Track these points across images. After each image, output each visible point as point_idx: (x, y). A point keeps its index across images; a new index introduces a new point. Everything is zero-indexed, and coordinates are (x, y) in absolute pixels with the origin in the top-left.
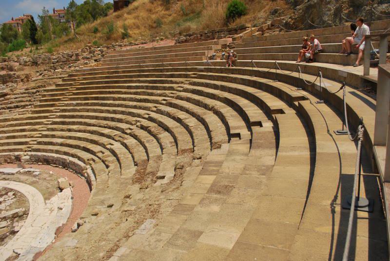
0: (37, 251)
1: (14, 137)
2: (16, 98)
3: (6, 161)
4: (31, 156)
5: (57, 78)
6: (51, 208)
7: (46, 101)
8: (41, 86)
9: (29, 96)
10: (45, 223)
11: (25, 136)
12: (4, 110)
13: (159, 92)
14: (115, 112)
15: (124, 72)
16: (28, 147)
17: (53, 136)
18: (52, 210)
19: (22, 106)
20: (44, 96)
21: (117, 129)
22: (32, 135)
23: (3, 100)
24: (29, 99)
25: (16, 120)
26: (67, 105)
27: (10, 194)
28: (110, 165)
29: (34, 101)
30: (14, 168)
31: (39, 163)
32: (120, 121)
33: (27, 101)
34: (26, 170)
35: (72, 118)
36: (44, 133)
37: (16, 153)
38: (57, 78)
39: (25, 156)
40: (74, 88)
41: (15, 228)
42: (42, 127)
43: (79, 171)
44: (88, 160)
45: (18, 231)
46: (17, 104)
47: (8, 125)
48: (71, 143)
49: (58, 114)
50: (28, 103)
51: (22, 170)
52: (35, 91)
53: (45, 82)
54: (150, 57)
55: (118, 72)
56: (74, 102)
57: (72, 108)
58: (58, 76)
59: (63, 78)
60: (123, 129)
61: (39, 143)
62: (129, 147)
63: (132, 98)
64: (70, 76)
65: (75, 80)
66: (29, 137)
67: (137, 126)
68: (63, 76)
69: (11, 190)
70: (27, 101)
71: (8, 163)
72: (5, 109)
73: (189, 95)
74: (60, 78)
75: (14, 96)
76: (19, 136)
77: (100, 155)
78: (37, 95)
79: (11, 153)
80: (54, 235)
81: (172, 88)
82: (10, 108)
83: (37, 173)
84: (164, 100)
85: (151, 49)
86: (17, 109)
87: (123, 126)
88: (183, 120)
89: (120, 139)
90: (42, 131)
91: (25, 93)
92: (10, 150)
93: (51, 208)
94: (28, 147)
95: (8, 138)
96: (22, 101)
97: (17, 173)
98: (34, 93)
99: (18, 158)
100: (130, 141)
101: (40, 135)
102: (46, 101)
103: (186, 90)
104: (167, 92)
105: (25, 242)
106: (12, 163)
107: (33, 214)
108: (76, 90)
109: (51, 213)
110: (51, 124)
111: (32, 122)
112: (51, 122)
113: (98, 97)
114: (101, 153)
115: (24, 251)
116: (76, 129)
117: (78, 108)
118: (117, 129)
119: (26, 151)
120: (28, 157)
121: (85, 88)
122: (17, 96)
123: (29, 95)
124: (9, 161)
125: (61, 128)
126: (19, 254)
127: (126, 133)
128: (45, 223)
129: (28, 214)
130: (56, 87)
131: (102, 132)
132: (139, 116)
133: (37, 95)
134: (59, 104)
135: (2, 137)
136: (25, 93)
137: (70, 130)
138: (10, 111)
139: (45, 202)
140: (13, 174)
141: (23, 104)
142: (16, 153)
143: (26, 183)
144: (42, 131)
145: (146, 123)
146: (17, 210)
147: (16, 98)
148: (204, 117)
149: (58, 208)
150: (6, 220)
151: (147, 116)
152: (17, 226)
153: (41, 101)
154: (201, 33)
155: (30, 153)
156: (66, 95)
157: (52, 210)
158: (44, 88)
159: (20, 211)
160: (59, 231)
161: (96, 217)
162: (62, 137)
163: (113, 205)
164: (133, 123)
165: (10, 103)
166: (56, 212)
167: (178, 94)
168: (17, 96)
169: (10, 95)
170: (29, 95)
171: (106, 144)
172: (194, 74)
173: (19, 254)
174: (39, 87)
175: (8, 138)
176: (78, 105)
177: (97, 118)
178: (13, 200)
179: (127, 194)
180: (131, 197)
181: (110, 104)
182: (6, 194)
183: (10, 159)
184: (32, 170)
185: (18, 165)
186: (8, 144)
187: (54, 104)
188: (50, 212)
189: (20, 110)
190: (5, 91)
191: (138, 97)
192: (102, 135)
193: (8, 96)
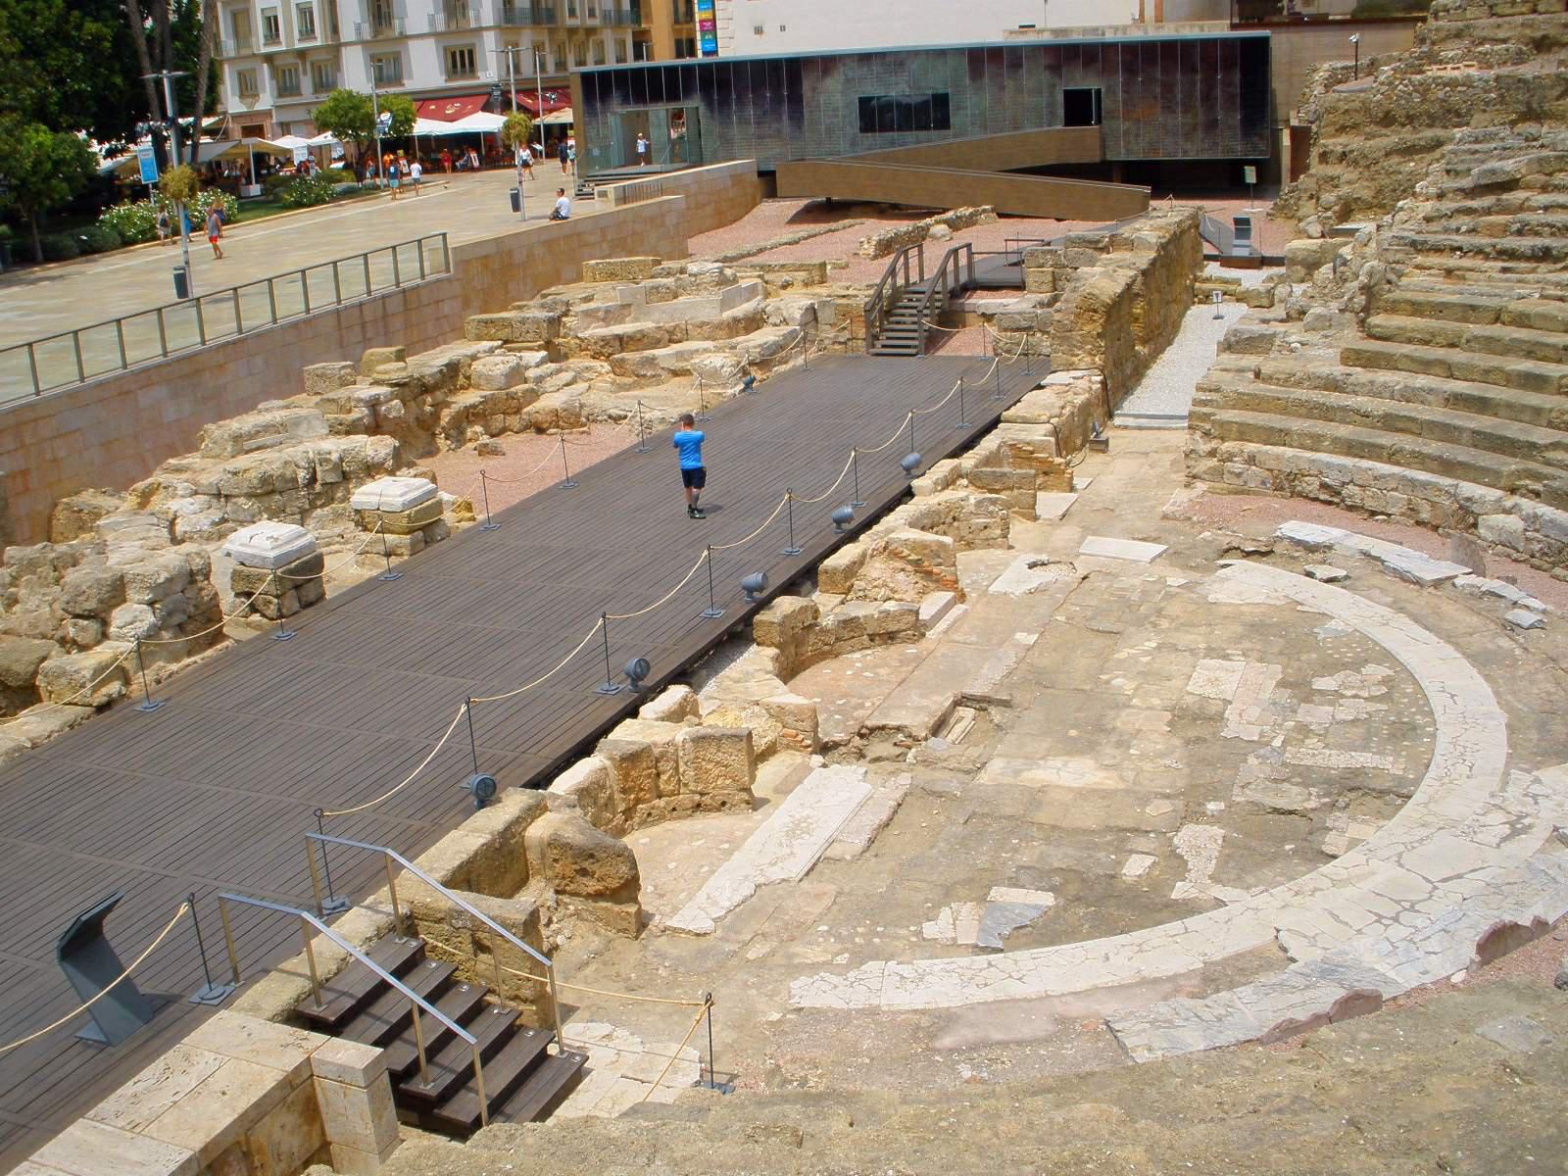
0: (1365, 986)
1: (1482, 405)
4: (1532, 519)
6: (1520, 817)
10: (1460, 876)
12: (1478, 262)
16: (1537, 476)
18: (1517, 828)
23: (1488, 211)
25: (1522, 320)
27: (1375, 671)
30: (1434, 556)
31: (1558, 571)
39: (1508, 512)
41: (1330, 837)
45: (1334, 857)
46: (1547, 241)
51: (1465, 579)
66: (1550, 425)
69: (1386, 656)
71: (1418, 523)
72: (1487, 257)
76: (1509, 406)
79: (1446, 481)
80: (1470, 952)
82: (1512, 255)
83: (1526, 618)
86: (1543, 267)
92: (1447, 467)
93: (1520, 817)
94: (1537, 476)
97: (1437, 584)
99: (1467, 517)
105: (1336, 918)
106: (1435, 528)
107: (1426, 805)
115: (1318, 954)
119: (1513, 491)
120: (1514, 523)
124: (1425, 516)
126: (1293, 960)
128: (1460, 876)
129: (1410, 797)
135: (1431, 391)
139: (1506, 774)
142: (1468, 489)
143: (1457, 646)
149: (1556, 829)
150: (1306, 785)
152: (1346, 830)
155: (1528, 505)
157: (1517, 828)
159: (1388, 764)
160: (1499, 941)
165: (1520, 233)
166: (1538, 845)
169: (1528, 187)
173: (1293, 960)
175: (1456, 400)
178: (1372, 707)
182: (1357, 665)
183: (1433, 505)
184: (1511, 592)
186: (1447, 432)
188: (1507, 830)
190: (1509, 165)
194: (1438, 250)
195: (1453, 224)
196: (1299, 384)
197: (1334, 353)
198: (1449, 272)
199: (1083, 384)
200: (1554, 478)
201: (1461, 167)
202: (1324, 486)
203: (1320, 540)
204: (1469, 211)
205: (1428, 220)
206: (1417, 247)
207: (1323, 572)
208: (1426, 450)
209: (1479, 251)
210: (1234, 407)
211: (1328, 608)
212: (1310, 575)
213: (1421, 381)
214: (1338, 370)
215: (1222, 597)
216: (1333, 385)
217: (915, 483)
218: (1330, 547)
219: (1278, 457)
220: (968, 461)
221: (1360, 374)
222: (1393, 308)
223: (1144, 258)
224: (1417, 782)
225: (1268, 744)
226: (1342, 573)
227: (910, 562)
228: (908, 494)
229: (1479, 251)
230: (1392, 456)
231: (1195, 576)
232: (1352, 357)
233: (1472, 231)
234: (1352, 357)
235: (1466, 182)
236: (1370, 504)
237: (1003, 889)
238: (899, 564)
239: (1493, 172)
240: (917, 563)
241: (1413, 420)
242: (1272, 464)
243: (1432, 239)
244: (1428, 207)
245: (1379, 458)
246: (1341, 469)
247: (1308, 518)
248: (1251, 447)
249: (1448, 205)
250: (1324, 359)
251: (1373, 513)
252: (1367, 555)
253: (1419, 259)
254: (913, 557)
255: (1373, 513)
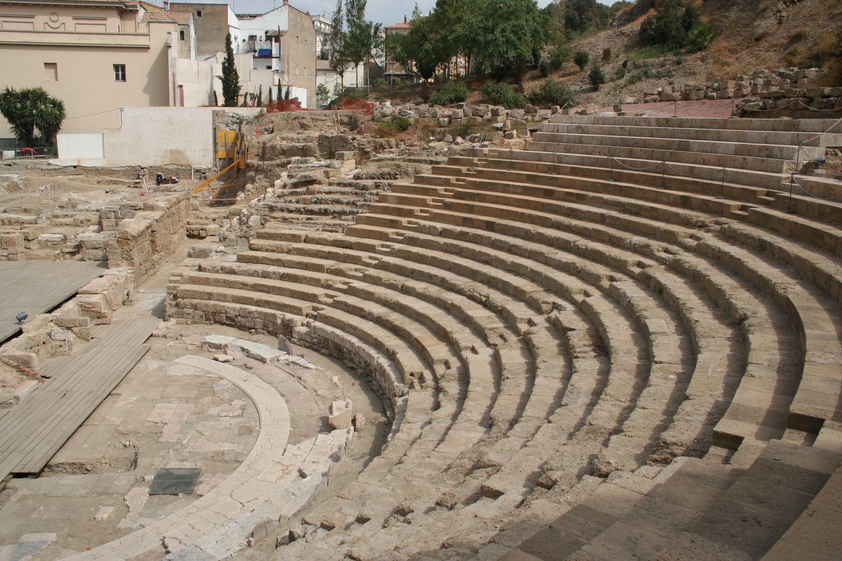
2: (329, 193)
3: (265, 327)
5: (425, 162)
7: (386, 210)
8: (389, 174)
9: (356, 194)
11: (316, 283)
13: (637, 239)
14: (516, 270)
15: (574, 172)
17: (368, 296)
18: (286, 472)
19: (334, 212)
20: (383, 199)
21: (502, 314)
22: (330, 282)
24: (352, 198)
26: (421, 229)
28: (442, 404)
29: (362, 206)
32: (518, 295)
33: (347, 204)
34: (292, 358)
35: (419, 262)
36: (357, 284)
37: (288, 316)
38: (425, 162)
39: (303, 325)
40: (451, 191)
42: (356, 270)
43: (382, 397)
44: (412, 374)
47: (295, 249)
48: (397, 323)
49: (397, 246)
50: (348, 209)
51: (283, 356)
52: (370, 183)
53: (398, 166)
54: (645, 144)
55: (556, 170)
56: (439, 226)
57: (429, 237)
58: (431, 158)
59: (438, 163)
60: (515, 319)
61: (337, 305)
62: (505, 373)
63: (568, 242)
64: (453, 161)
65: (458, 173)
67: (548, 320)
68: (440, 158)
70: (347, 204)
72: (301, 213)
73: (701, 265)
74: (431, 162)
75: (326, 188)
77: (440, 369)
78: (371, 194)
79: (279, 313)
81: (670, 237)
82: (312, 212)
84: (640, 265)
85: (658, 122)
86: (324, 217)
87: (519, 310)
88: (653, 337)
89: (499, 341)
90: (353, 277)
91: (350, 185)
94: (315, 309)
95: (283, 277)
96: (338, 202)
98: (364, 188)
100: (513, 357)
101: (345, 287)
102: (386, 210)
103: (702, 251)
104: (655, 244)
108: (454, 197)
109: (282, 477)
110: (376, 267)
111: (343, 253)
112: (376, 262)
113: (492, 223)
114: (443, 367)
116: (420, 291)
117: (442, 240)
118: (502, 314)
121: (472, 197)
122: (334, 188)
123: (358, 191)
124: (271, 329)
125: (392, 281)
127: (517, 332)
130: (416, 182)
131: (470, 313)
132: (563, 292)
133: (371, 194)
134: (409, 222)
135: (274, 273)
136: (350, 185)
137: (406, 291)
138: (308, 219)
140: (263, 360)
141: (338, 208)
142: (288, 316)
144: (353, 277)
145: (568, 316)
146: (227, 447)
147: (329, 193)
148: (702, 343)
151: (580, 298)
153: (372, 209)
154: (811, 94)
156: (428, 206)
158: (390, 181)
161: (327, 532)
162: (385, 303)
163: (367, 520)
164: (544, 307)
165: (316, 203)
167: (678, 257)
168: (334, 188)
169: (320, 183)
170: (358, 191)
171: (463, 344)
172: (743, 208)
174: (382, 176)
175: (283, 277)
176: (444, 233)
177: (473, 275)
179: (406, 505)
180: (409, 516)
181: (513, 245)
184: (302, 361)
185: (280, 343)
187: (396, 222)
189: (328, 222)
191: (582, 242)
192: (466, 320)
193: (316, 187)
194: (282, 210)
195: (289, 198)
196: (217, 272)
197: (235, 258)
198: (285, 220)
199: (124, 274)
200: (322, 309)
201: (294, 174)
202: (228, 318)
203: (223, 343)
204: (296, 193)
205: (279, 197)
206: (272, 209)
207: (222, 357)
208: (270, 299)
209: (298, 211)
210: (188, 283)
211: (223, 374)
212: (216, 359)
213: (271, 269)
214: (235, 266)
215: (172, 373)
216: (232, 272)
217: (24, 326)
218: (226, 346)
219: (206, 305)
220: (57, 313)
221: (245, 266)
222: (260, 236)
223: (157, 215)
224: (246, 455)
225: (181, 443)
226: (230, 358)
227: (14, 367)
228: (20, 333)
229: (298, 211)
230: (258, 303)
231: (162, 363)
232: (241, 259)
233: (298, 202)
234: (241, 259)
235: (294, 181)
236: (247, 324)
237: (29, 535)
238: (8, 368)
239: (306, 176)
240: (16, 367)
241: (266, 286)
242: (204, 308)
243: (279, 205)
244: (279, 191)
245: (252, 304)
246: (234, 309)
247: (218, 333)
248: (195, 301)
249: (287, 191)
250: (230, 261)
251: (250, 329)
252: (243, 350)
253: (275, 214)
254: (15, 364)
255: (250, 329)
